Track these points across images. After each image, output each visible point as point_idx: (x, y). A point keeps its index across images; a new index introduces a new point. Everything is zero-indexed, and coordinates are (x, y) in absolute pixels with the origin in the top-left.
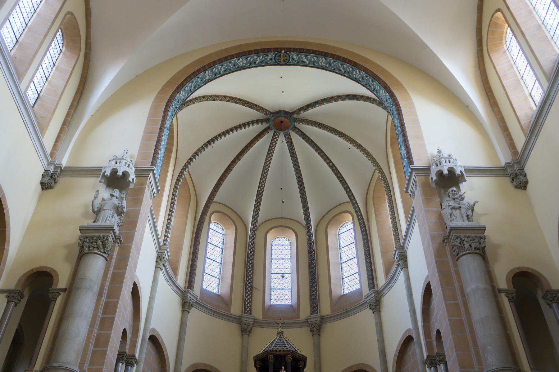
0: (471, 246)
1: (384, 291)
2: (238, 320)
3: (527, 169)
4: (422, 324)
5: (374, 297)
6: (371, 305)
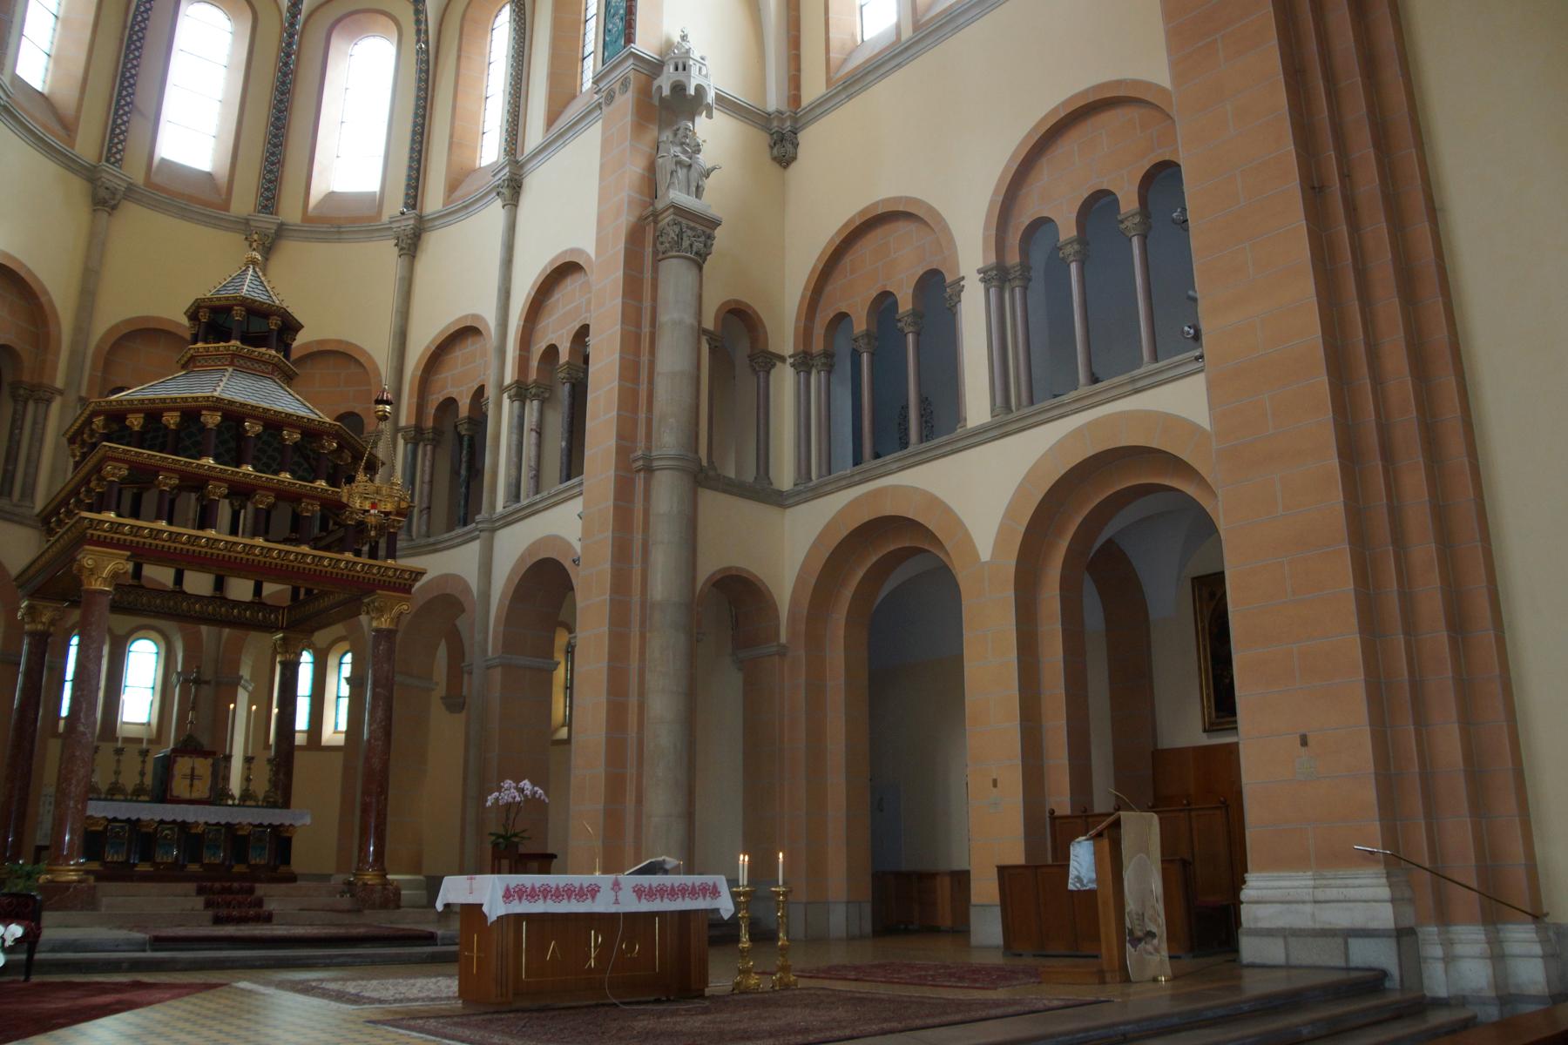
0: (691, 245)
1: (436, 223)
2: (90, 174)
3: (804, 137)
4: (522, 323)
5: (411, 226)
6: (400, 240)
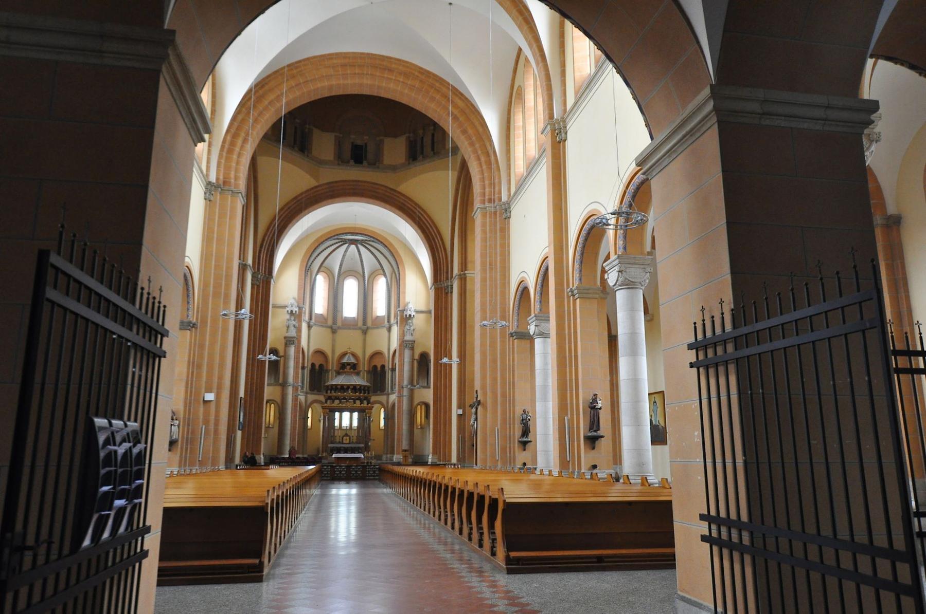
2: (331, 327)
